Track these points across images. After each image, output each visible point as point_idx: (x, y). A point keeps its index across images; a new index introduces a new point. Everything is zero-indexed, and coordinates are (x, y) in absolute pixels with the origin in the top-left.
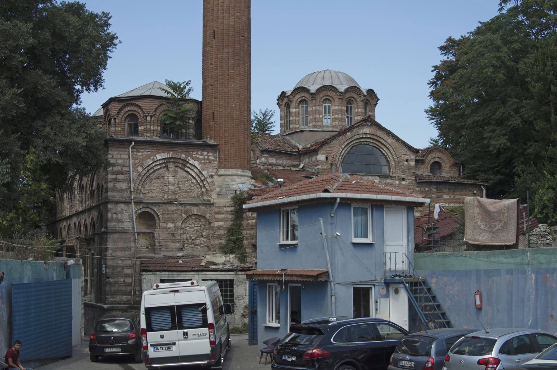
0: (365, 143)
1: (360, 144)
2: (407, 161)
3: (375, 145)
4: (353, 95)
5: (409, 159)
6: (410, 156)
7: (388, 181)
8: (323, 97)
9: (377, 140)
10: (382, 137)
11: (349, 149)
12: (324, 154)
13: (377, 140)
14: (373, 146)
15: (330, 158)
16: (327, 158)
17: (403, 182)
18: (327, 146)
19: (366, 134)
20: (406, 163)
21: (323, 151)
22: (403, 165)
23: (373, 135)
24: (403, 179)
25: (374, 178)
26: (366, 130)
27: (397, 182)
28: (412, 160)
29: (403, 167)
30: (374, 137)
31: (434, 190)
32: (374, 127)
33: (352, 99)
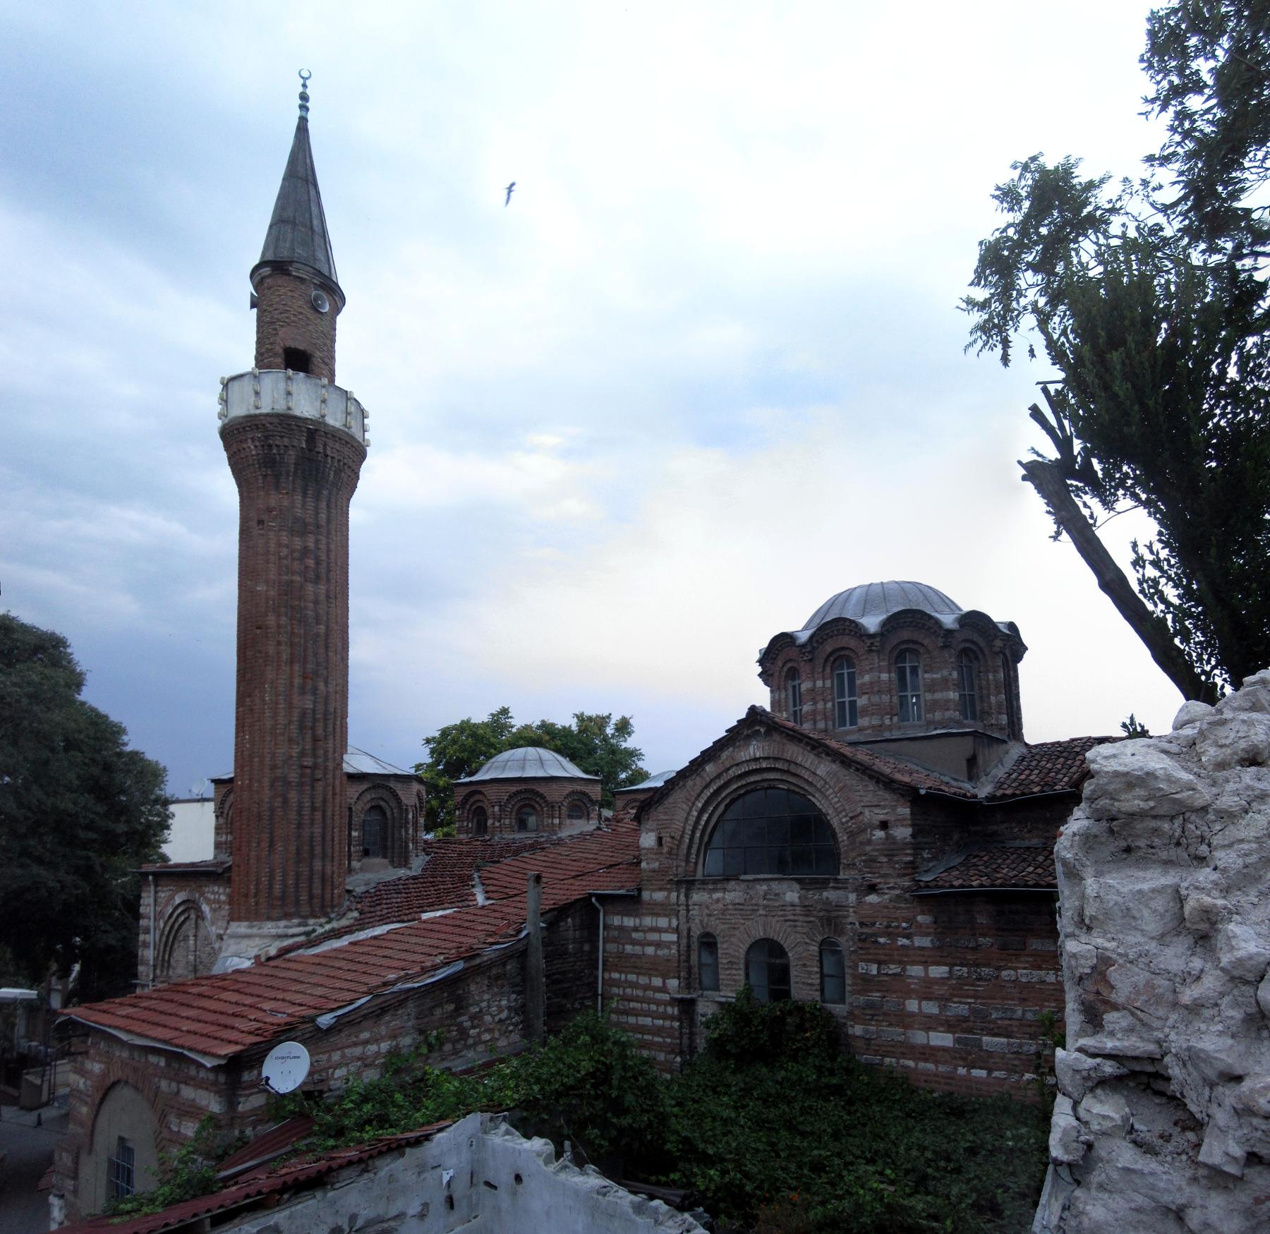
0: (766, 784)
1: (752, 789)
2: (884, 825)
3: (793, 788)
4: (906, 634)
5: (891, 818)
6: (894, 808)
7: (825, 894)
8: (784, 665)
9: (788, 772)
10: (799, 760)
11: (722, 807)
12: (652, 831)
13: (788, 772)
14: (788, 790)
15: (666, 840)
16: (660, 840)
17: (872, 898)
18: (661, 809)
19: (756, 760)
20: (880, 834)
21: (650, 824)
22: (869, 842)
23: (776, 759)
24: (872, 888)
25: (785, 885)
26: (754, 749)
27: (852, 897)
28: (900, 822)
29: (868, 848)
30: (779, 765)
31: (982, 920)
32: (776, 737)
33: (847, 653)
